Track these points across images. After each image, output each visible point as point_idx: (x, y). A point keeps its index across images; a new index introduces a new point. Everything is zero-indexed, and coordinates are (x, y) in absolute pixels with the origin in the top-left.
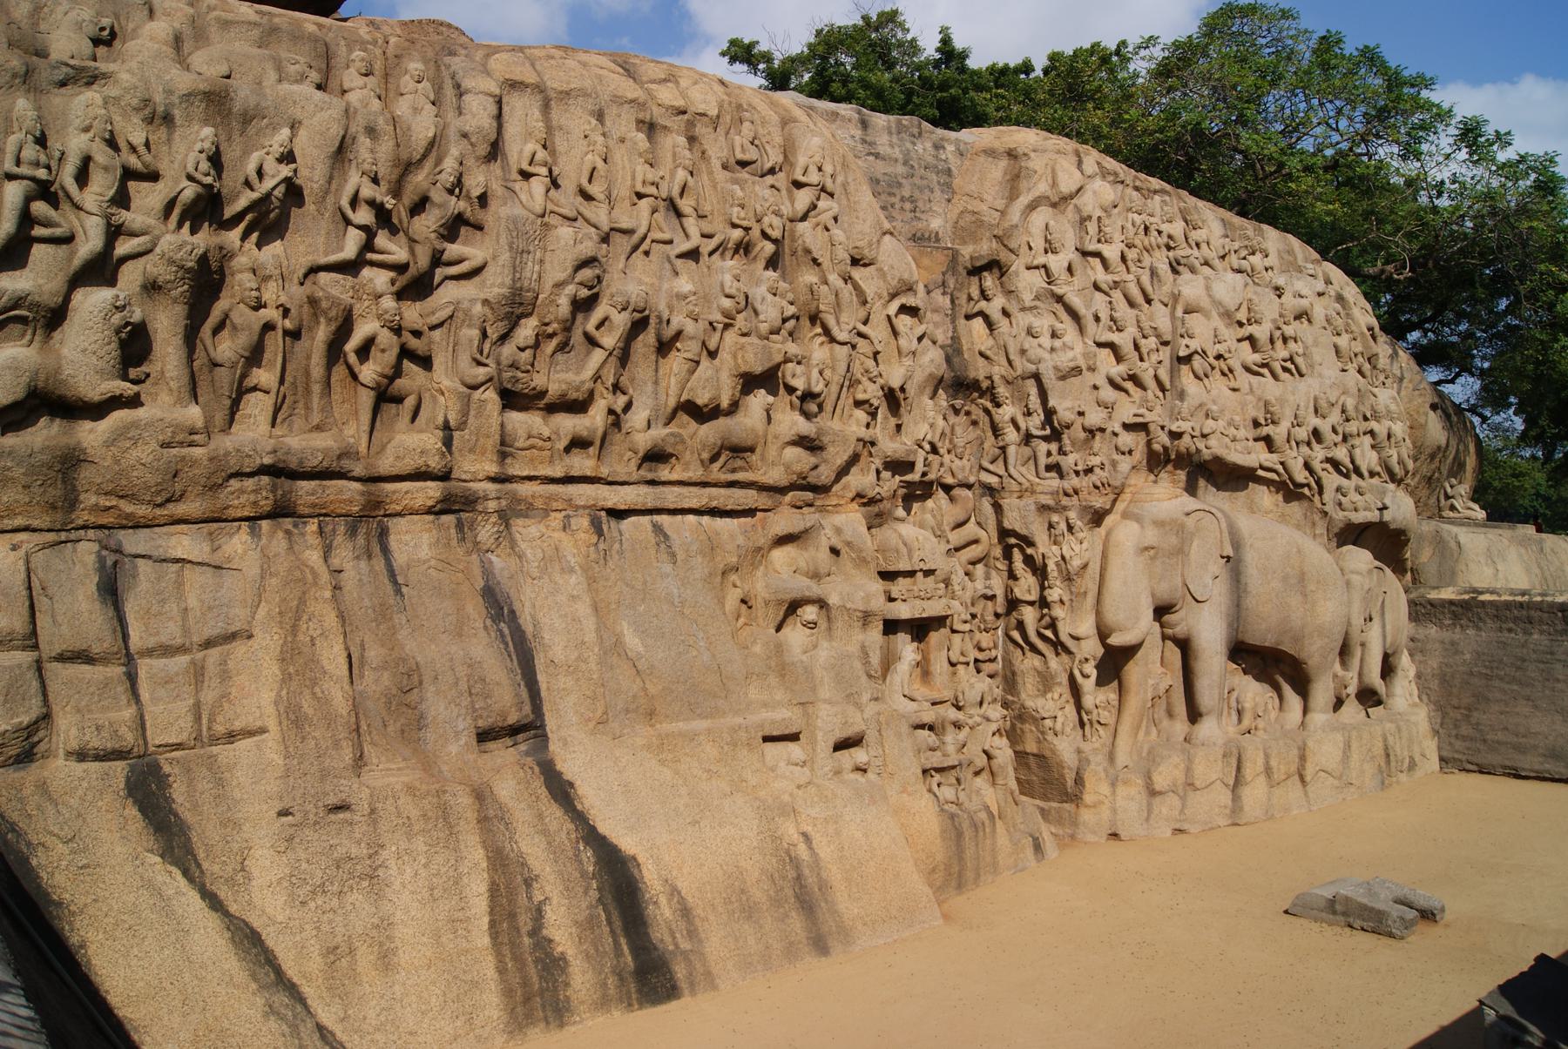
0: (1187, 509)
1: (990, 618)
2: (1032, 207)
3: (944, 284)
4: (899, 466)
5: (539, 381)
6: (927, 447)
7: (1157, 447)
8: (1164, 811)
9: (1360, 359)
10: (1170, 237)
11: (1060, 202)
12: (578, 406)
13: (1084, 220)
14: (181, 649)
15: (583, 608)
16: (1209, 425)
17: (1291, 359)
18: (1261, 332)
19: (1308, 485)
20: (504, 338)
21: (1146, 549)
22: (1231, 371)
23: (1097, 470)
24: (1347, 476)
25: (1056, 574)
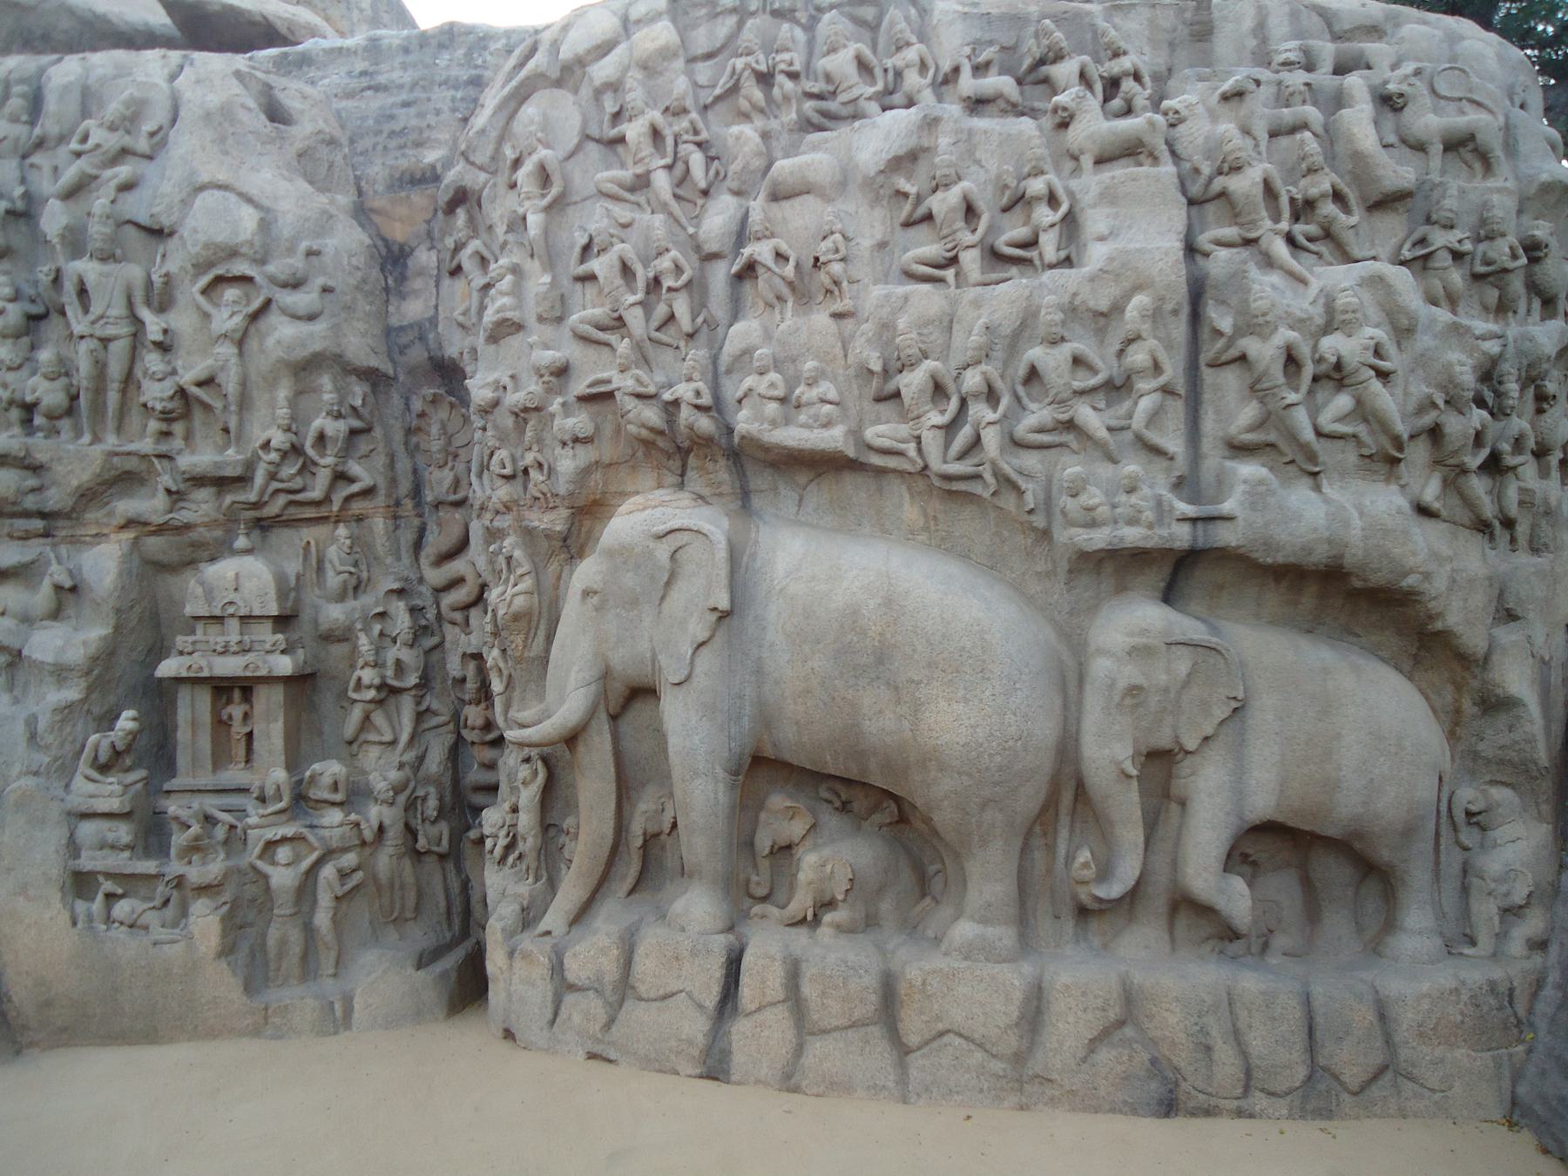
0: (662, 528)
1: (471, 685)
2: (520, 97)
3: (429, 234)
4: (222, 483)
6: (274, 456)
7: (632, 428)
8: (577, 1019)
9: (1329, 208)
10: (828, 78)
11: (568, 74)
13: (598, 93)
16: (749, 381)
17: (1032, 243)
18: (944, 203)
21: (587, 593)
23: (533, 474)
24: (1114, 461)
25: (488, 628)
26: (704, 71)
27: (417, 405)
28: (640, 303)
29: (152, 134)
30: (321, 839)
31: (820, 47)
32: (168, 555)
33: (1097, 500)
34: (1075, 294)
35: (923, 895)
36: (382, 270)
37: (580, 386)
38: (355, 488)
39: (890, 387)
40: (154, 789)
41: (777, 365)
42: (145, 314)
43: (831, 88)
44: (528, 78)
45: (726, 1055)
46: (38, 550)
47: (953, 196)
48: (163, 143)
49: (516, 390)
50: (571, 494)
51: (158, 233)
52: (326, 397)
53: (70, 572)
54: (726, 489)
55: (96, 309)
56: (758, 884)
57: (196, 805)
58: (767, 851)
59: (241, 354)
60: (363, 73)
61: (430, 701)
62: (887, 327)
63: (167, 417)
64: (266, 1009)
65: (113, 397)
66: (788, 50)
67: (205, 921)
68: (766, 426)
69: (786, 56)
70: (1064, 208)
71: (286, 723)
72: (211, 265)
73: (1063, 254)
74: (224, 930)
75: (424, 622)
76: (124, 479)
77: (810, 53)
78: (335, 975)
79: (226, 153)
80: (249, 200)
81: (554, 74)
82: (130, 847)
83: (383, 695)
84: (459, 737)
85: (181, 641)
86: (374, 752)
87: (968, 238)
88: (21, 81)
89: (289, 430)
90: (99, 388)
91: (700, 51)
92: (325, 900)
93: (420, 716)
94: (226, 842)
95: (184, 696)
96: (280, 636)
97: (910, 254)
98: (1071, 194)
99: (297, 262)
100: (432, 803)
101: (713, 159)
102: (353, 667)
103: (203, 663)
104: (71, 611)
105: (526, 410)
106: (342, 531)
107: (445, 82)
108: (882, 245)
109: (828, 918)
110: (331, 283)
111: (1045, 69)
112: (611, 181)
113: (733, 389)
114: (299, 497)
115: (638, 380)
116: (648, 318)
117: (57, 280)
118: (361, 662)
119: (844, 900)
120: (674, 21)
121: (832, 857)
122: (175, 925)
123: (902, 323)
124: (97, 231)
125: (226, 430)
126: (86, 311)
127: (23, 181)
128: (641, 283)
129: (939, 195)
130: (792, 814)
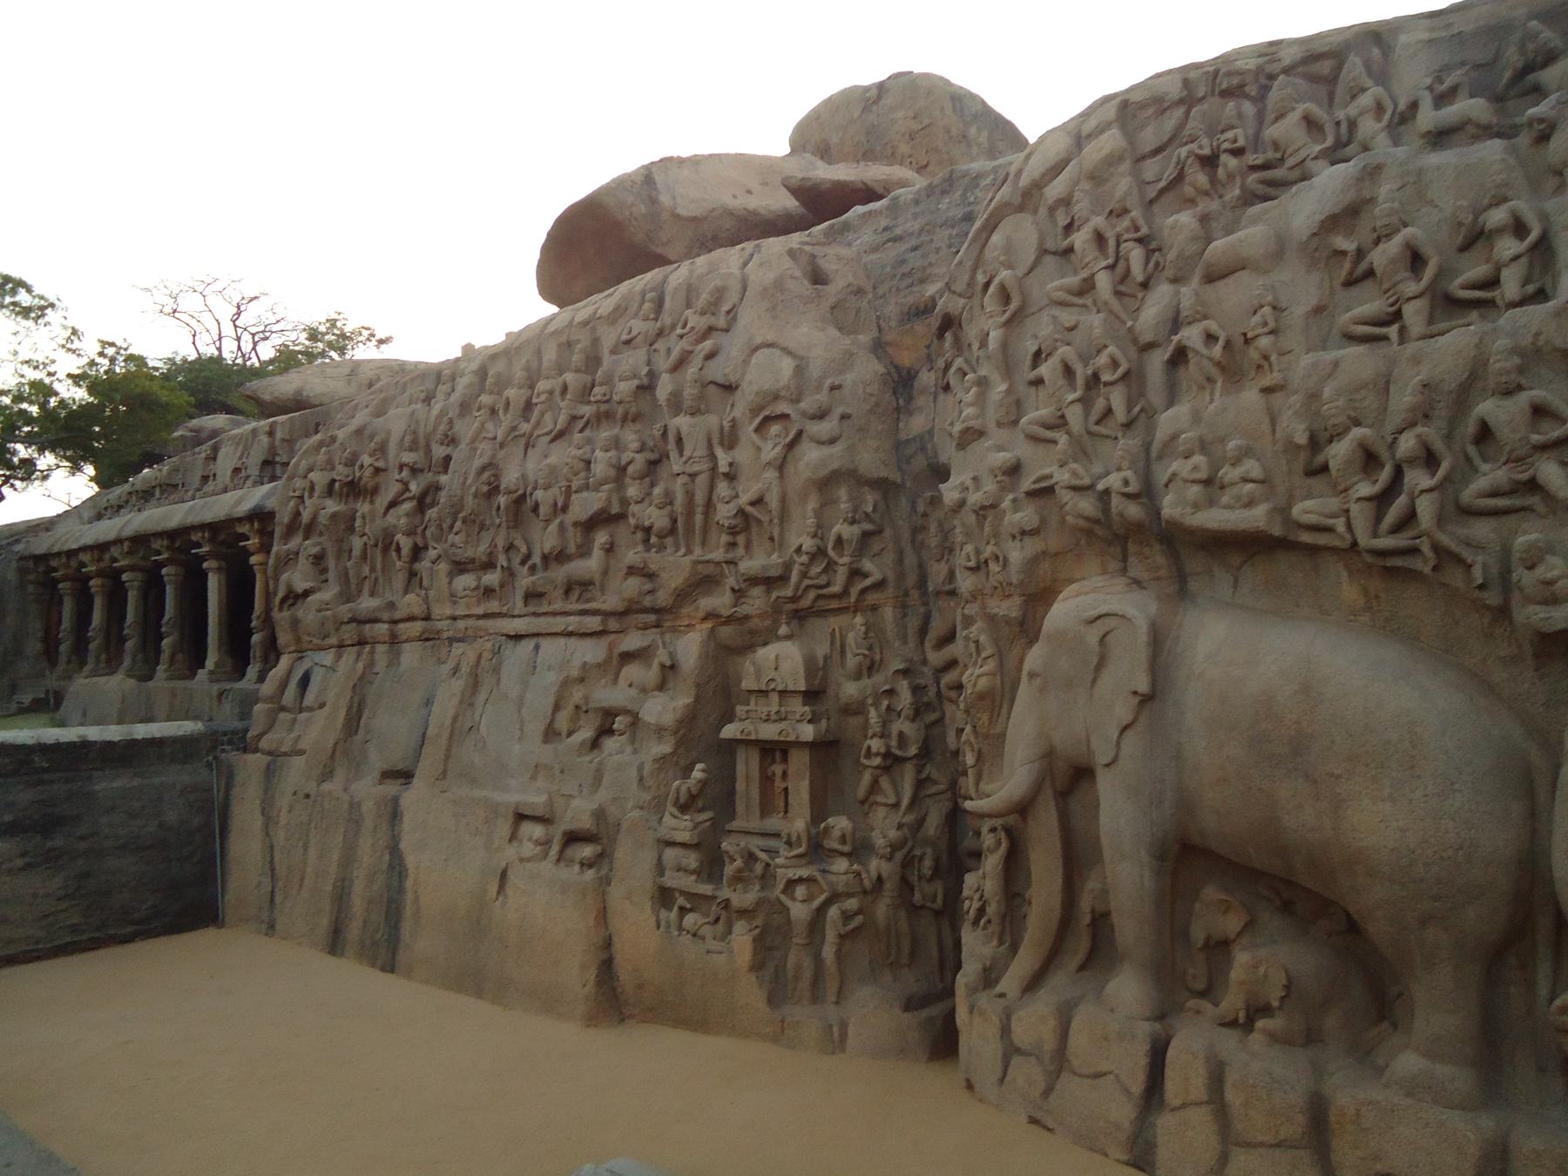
2: (990, 227)
4: (769, 582)
5: (470, 553)
6: (804, 559)
10: (1276, 145)
12: (489, 565)
13: (1052, 210)
14: (310, 709)
15: (456, 700)
18: (1383, 256)
19: (1413, 551)
20: (452, 527)
21: (1032, 675)
22: (1266, 358)
26: (1151, 168)
27: (921, 508)
28: (1079, 400)
29: (728, 312)
30: (830, 884)
31: (1270, 116)
32: (733, 643)
33: (1555, 573)
34: (1538, 334)
35: (1382, 1018)
36: (895, 393)
37: (1027, 484)
38: (868, 582)
39: (1320, 459)
40: (718, 829)
41: (1203, 446)
42: (719, 452)
43: (1278, 155)
44: (995, 209)
45: (1150, 1147)
46: (651, 637)
47: (1393, 246)
48: (734, 319)
49: (977, 489)
50: (1022, 583)
51: (729, 388)
52: (842, 506)
53: (670, 654)
54: (1163, 572)
55: (687, 453)
56: (1194, 977)
57: (743, 844)
58: (1200, 944)
59: (781, 476)
60: (886, 229)
61: (930, 770)
62: (1314, 396)
63: (733, 531)
64: (783, 1021)
65: (699, 518)
66: (1233, 128)
67: (742, 939)
68: (1189, 510)
69: (1230, 135)
70: (1534, 236)
71: (811, 782)
72: (762, 408)
73: (1530, 289)
74: (755, 949)
75: (925, 699)
76: (704, 582)
77: (1261, 123)
78: (837, 1003)
79: (774, 317)
80: (788, 352)
81: (1017, 200)
82: (697, 872)
83: (889, 762)
84: (956, 803)
85: (740, 710)
86: (881, 812)
87: (1411, 288)
88: (652, 290)
89: (815, 536)
90: (690, 513)
91: (1148, 149)
92: (831, 936)
93: (920, 784)
94: (763, 877)
95: (741, 756)
96: (807, 708)
97: (1348, 315)
98: (1544, 217)
99: (822, 397)
100: (928, 863)
101: (1154, 251)
102: (866, 736)
103: (751, 728)
104: (671, 685)
105: (983, 508)
106: (859, 619)
107: (944, 224)
108: (1319, 310)
109: (1260, 1024)
110: (849, 411)
111: (1531, 78)
112: (1060, 289)
113: (1161, 475)
114: (824, 591)
115: (1075, 474)
116: (1087, 414)
117: (665, 434)
118: (870, 733)
119: (1280, 1008)
120: (1123, 127)
121: (1265, 960)
122: (723, 939)
123: (1327, 392)
124: (689, 392)
125: (772, 539)
126: (681, 453)
127: (649, 363)
128: (1080, 381)
129: (1381, 247)
130: (1226, 908)
